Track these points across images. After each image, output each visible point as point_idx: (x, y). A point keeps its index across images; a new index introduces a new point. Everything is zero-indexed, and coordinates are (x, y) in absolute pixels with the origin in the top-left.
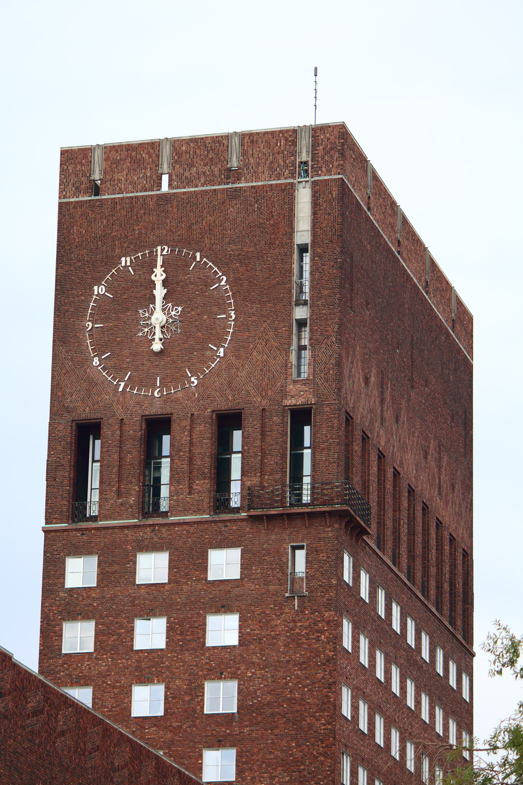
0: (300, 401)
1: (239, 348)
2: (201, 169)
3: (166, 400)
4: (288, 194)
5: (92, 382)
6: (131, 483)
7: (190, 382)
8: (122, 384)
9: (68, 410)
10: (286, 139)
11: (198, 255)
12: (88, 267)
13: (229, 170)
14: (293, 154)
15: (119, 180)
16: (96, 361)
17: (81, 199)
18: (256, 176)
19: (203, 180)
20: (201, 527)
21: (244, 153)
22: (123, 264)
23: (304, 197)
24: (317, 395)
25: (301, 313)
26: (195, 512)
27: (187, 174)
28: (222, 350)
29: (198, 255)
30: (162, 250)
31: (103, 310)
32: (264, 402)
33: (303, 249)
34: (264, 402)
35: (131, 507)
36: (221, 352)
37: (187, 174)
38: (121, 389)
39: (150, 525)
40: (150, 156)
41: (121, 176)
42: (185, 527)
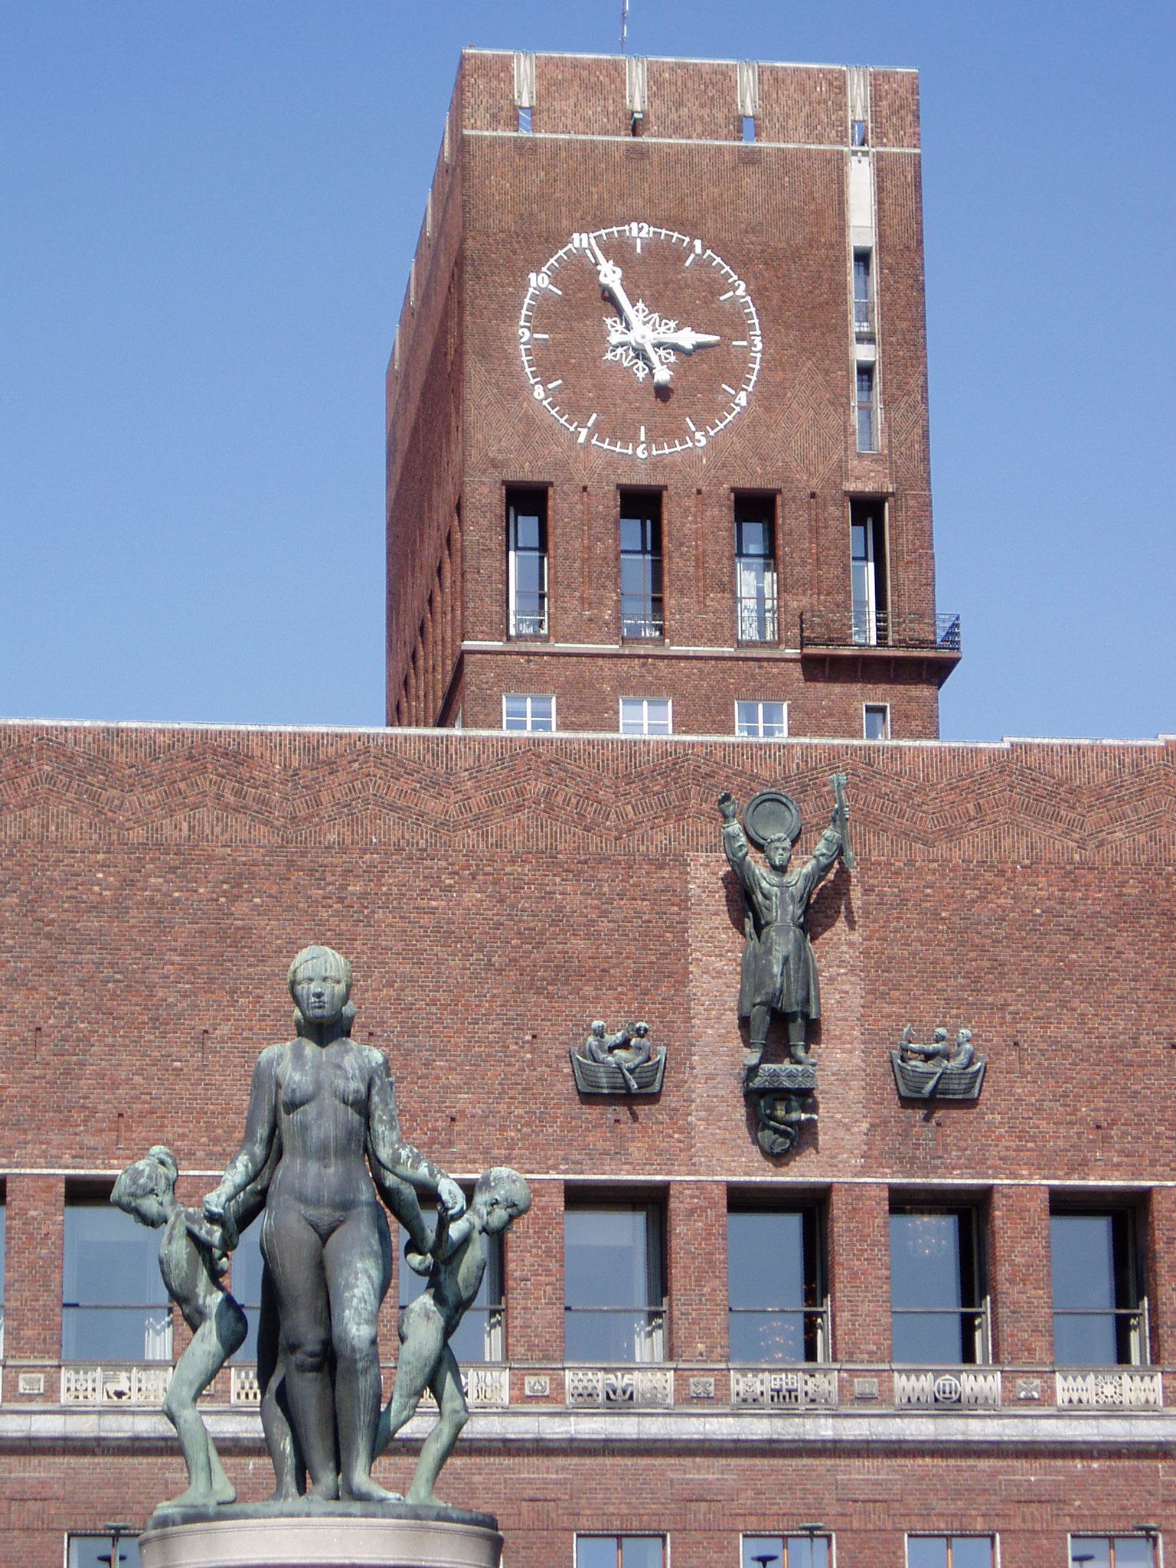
0: (869, 487)
1: (768, 397)
2: (696, 111)
3: (656, 463)
4: (837, 167)
5: (531, 425)
6: (604, 587)
7: (692, 439)
8: (584, 432)
9: (494, 464)
10: (830, 84)
11: (698, 243)
12: (518, 242)
13: (740, 119)
14: (841, 106)
15: (563, 113)
16: (539, 392)
17: (500, 133)
18: (783, 133)
19: (699, 129)
20: (721, 664)
21: (764, 96)
22: (577, 244)
23: (860, 179)
24: (896, 480)
25: (863, 353)
26: (711, 642)
27: (673, 116)
28: (743, 394)
29: (698, 243)
30: (640, 230)
31: (545, 314)
32: (814, 482)
33: (862, 257)
34: (814, 482)
35: (607, 624)
36: (742, 398)
37: (673, 116)
38: (581, 439)
39: (639, 657)
40: (612, 81)
41: (568, 106)
42: (699, 664)
